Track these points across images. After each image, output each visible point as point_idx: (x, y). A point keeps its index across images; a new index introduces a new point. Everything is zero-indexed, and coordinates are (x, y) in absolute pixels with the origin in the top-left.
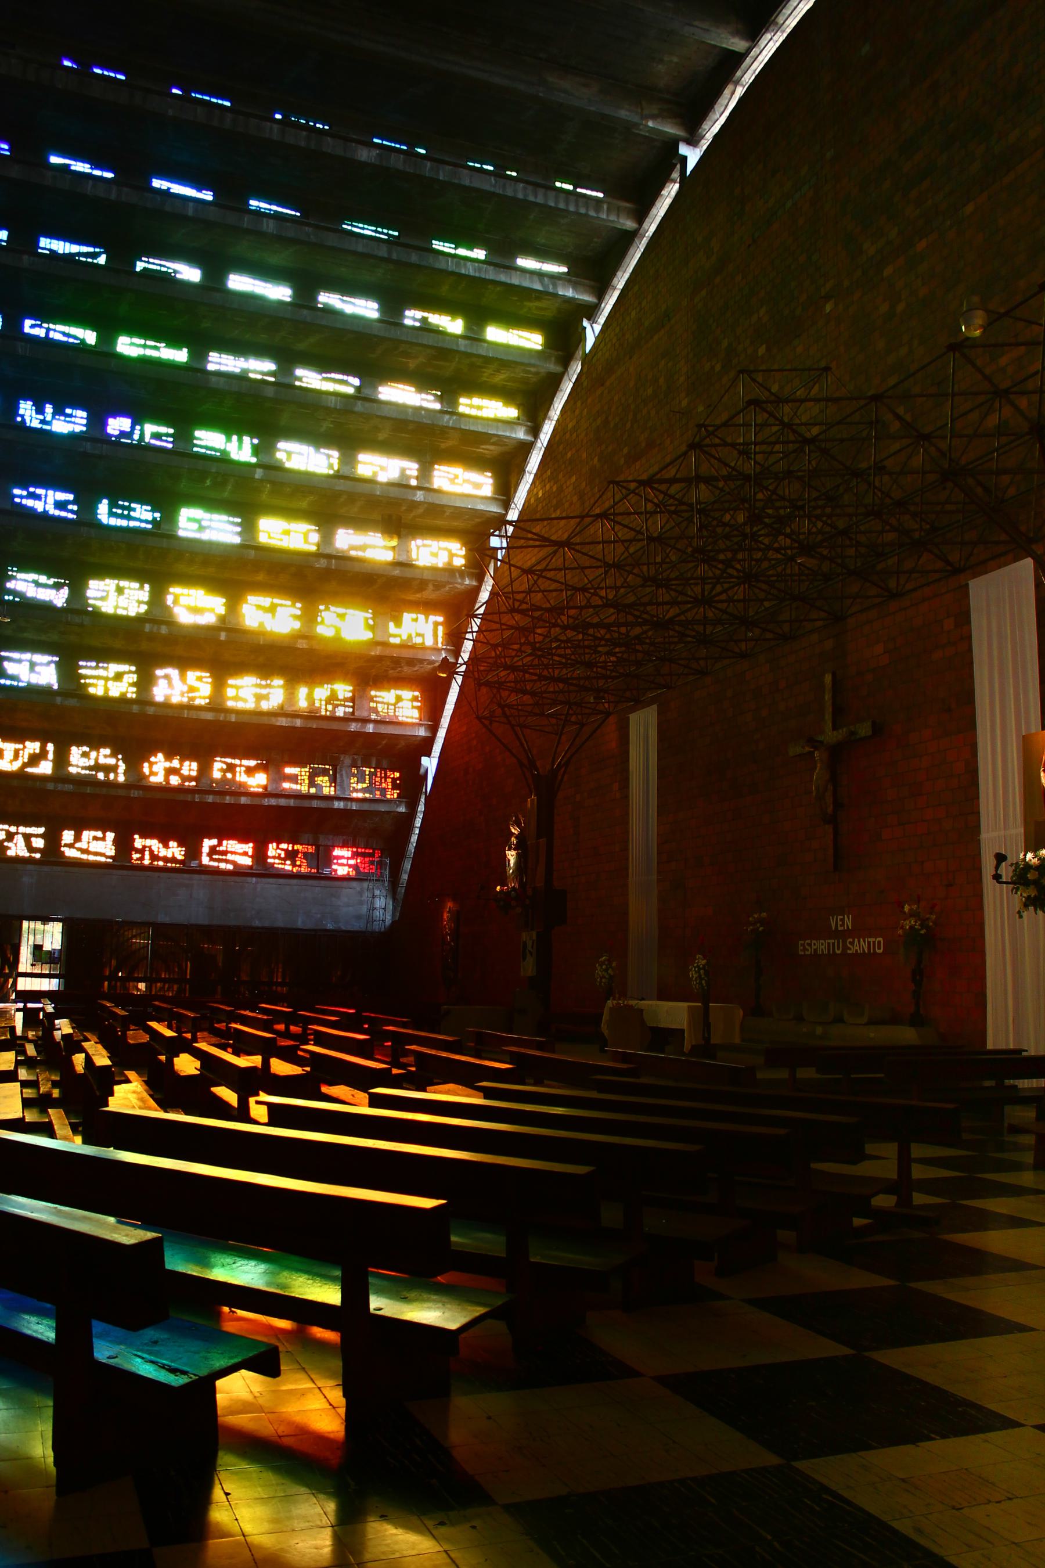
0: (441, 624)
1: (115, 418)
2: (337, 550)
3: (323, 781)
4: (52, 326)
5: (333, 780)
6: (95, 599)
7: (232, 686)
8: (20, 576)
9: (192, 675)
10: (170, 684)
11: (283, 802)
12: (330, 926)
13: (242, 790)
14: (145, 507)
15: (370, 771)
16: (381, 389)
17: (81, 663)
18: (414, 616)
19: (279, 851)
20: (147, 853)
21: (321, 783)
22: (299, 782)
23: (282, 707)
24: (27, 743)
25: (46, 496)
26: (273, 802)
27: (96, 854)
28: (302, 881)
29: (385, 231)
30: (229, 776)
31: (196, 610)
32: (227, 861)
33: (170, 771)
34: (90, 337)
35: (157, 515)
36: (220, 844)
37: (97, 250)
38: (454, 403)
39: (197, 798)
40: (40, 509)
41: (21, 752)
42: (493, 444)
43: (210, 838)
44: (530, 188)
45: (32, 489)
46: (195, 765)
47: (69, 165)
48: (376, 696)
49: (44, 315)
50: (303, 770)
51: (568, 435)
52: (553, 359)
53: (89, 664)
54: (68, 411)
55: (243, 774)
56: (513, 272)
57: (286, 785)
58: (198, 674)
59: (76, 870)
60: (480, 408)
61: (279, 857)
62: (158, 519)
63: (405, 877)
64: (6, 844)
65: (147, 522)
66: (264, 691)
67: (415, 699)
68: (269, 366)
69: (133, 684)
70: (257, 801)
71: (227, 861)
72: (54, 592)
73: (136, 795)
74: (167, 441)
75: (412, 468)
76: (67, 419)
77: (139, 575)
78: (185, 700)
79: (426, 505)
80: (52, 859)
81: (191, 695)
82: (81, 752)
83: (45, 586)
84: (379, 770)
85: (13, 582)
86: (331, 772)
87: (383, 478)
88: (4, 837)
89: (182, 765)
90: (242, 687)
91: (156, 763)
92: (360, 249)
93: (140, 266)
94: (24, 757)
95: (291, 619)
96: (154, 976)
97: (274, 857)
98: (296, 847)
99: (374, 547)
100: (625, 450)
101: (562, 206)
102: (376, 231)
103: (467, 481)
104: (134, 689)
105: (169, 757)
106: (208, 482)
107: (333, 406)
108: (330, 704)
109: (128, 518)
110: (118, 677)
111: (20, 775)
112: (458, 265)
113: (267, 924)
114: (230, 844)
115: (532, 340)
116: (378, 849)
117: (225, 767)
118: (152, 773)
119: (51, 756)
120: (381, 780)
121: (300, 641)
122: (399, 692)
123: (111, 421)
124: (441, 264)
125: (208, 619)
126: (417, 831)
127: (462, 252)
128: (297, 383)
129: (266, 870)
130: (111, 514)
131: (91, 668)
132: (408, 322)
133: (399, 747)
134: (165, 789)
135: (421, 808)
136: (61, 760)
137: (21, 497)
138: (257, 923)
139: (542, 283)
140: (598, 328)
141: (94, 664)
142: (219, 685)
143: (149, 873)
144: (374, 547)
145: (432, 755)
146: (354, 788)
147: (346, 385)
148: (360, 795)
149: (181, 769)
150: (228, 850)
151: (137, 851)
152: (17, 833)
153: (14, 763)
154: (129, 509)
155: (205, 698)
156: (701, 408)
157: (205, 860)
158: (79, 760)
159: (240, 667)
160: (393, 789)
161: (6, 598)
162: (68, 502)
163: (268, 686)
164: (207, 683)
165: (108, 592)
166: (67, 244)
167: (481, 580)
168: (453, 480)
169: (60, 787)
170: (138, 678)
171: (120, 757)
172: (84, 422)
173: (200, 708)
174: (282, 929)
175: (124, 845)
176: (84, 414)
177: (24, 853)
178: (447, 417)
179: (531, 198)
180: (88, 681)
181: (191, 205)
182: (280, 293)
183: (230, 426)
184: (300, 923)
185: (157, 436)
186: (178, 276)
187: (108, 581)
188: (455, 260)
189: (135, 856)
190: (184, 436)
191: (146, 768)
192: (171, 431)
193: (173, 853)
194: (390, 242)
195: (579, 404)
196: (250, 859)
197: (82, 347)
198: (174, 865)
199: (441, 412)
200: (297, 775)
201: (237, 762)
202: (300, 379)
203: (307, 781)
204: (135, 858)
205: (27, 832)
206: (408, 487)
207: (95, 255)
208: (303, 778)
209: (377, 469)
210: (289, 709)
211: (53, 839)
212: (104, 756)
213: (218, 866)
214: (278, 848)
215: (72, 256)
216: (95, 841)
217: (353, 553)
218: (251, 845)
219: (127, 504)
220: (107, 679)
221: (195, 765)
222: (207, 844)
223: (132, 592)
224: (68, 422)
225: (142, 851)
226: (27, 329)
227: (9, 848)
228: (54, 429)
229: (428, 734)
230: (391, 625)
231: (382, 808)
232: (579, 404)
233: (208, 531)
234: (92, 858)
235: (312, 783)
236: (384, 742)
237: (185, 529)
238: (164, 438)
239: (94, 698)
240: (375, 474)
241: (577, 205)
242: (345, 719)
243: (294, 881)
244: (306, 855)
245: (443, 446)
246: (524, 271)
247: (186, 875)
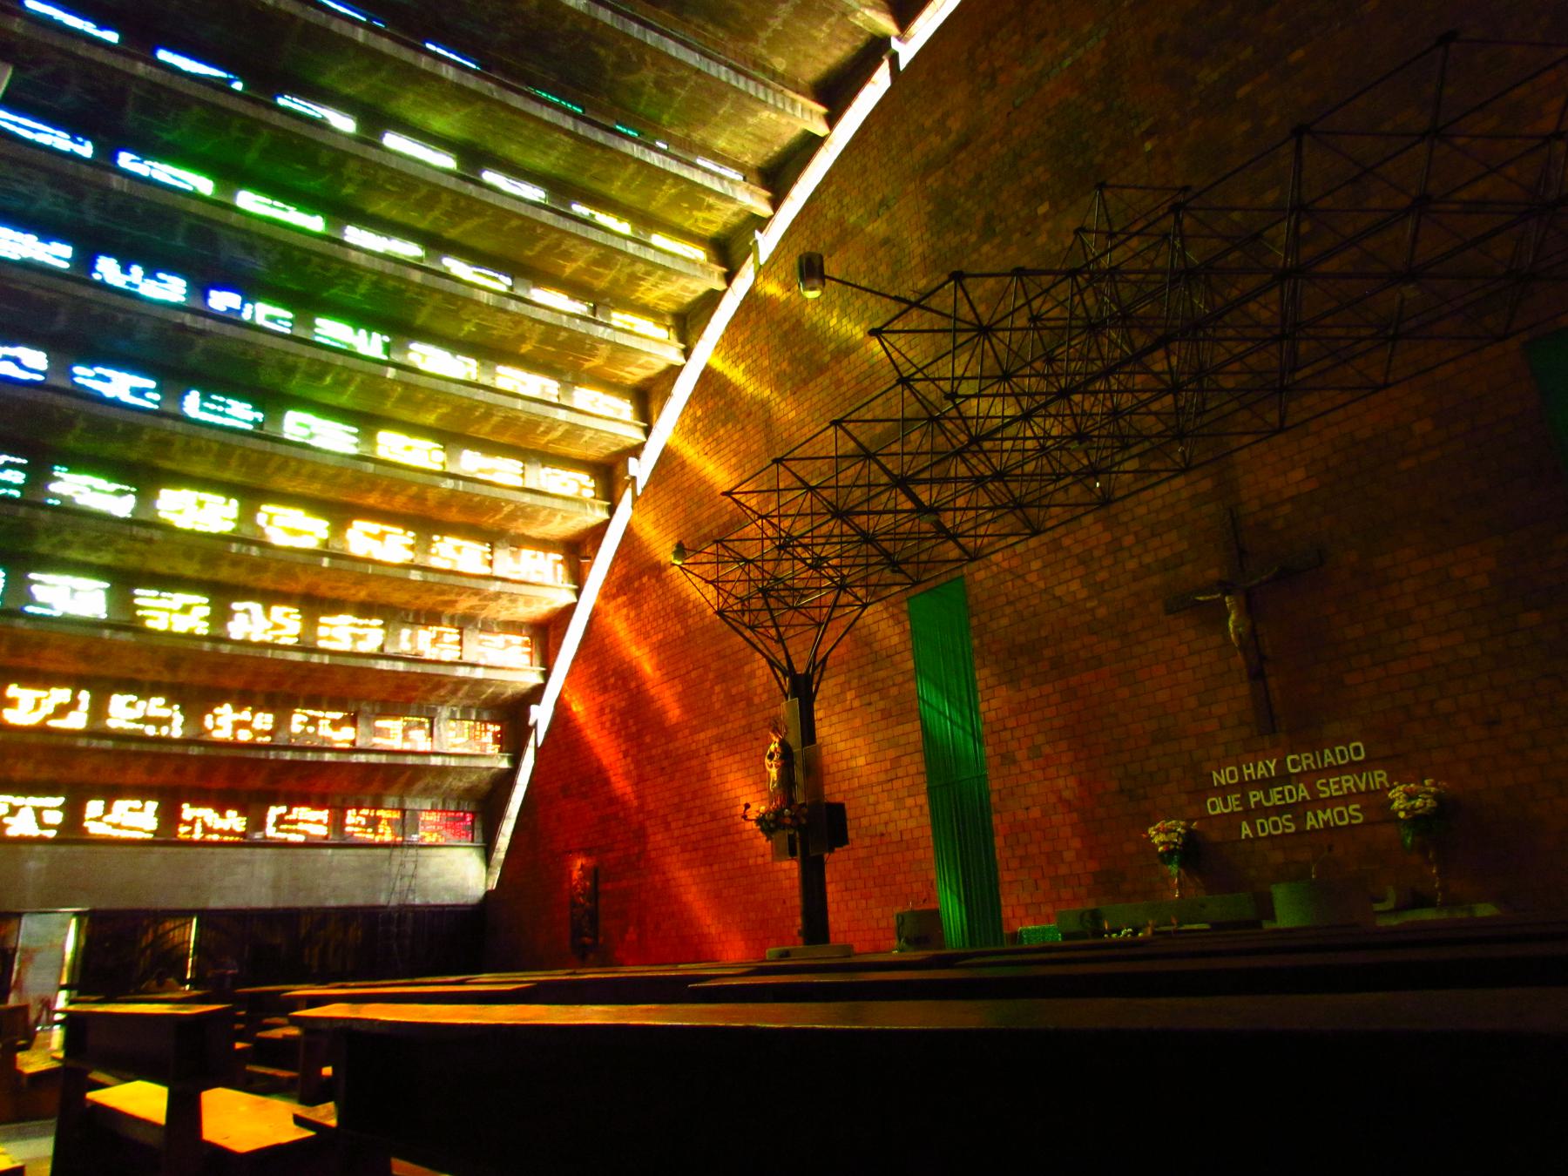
0: (562, 562)
4: (156, 164)
9: (278, 611)
11: (373, 758)
12: (418, 901)
13: (326, 745)
19: (359, 818)
24: (54, 691)
26: (362, 758)
27: (131, 829)
31: (295, 533)
34: (204, 185)
35: (260, 416)
36: (289, 812)
39: (272, 755)
41: (43, 702)
43: (277, 803)
44: (732, 73)
45: (100, 370)
49: (146, 150)
52: (716, 275)
54: (161, 276)
56: (695, 170)
59: (102, 848)
61: (359, 825)
69: (207, 619)
70: (343, 758)
71: (297, 832)
79: (567, 427)
86: (427, 726)
94: (48, 708)
97: (354, 825)
101: (761, 96)
104: (207, 624)
105: (238, 707)
106: (328, 380)
107: (485, 301)
109: (223, 414)
110: (186, 609)
111: (42, 730)
113: (344, 902)
114: (301, 812)
118: (216, 727)
125: (310, 543)
130: (202, 408)
133: (506, 696)
134: (236, 745)
136: (99, 709)
137: (85, 377)
138: (332, 903)
139: (722, 185)
142: (310, 620)
143: (200, 849)
149: (251, 722)
154: (224, 405)
157: (271, 831)
158: (124, 712)
159: (336, 606)
163: (367, 626)
169: (95, 743)
171: (177, 707)
175: (169, 816)
177: (34, 831)
178: (601, 329)
179: (734, 83)
184: (382, 900)
185: (273, 319)
192: (289, 315)
196: (326, 828)
201: (319, 714)
203: (400, 735)
210: (389, 650)
211: (74, 813)
212: (156, 706)
214: (358, 814)
218: (326, 812)
220: (171, 611)
225: (192, 823)
231: (483, 763)
235: (406, 737)
236: (490, 690)
238: (280, 322)
241: (775, 99)
247: (247, 850)
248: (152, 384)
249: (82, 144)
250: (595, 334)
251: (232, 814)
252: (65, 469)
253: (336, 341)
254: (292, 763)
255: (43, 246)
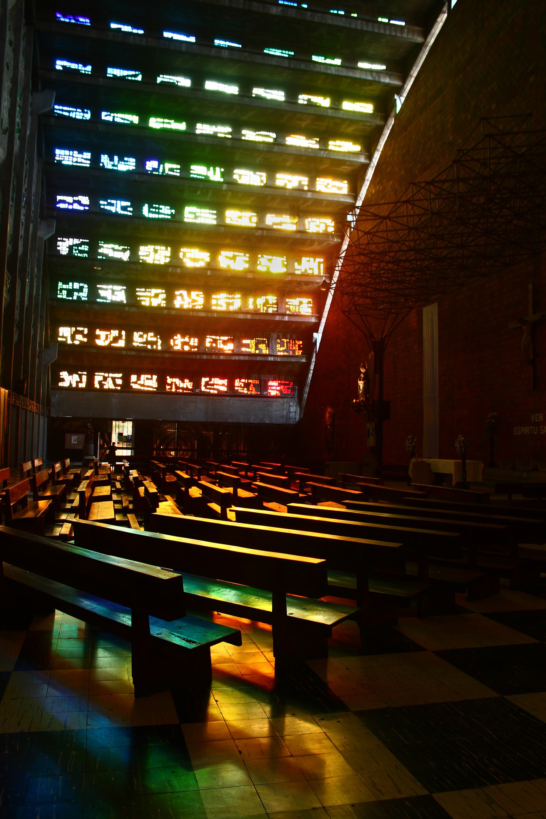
1: (150, 161)
2: (267, 226)
3: (262, 346)
4: (115, 115)
5: (268, 346)
6: (143, 256)
7: (214, 299)
8: (105, 246)
9: (194, 294)
10: (183, 299)
11: (242, 358)
12: (267, 422)
13: (221, 352)
14: (167, 207)
15: (287, 341)
16: (287, 139)
17: (137, 289)
18: (308, 259)
19: (240, 383)
20: (174, 386)
21: (261, 348)
22: (250, 347)
23: (240, 309)
24: (112, 331)
25: (116, 204)
26: (237, 358)
28: (253, 399)
29: (287, 52)
30: (214, 345)
31: (195, 260)
32: (214, 389)
33: (184, 344)
34: (135, 119)
35: (173, 211)
36: (210, 380)
37: (137, 73)
38: (327, 145)
39: (198, 357)
40: (114, 211)
41: (109, 336)
42: (348, 165)
43: (205, 378)
45: (109, 201)
46: (196, 340)
47: (120, 28)
48: (289, 302)
49: (112, 109)
50: (252, 341)
51: (387, 159)
52: (379, 118)
53: (141, 290)
54: (126, 159)
55: (221, 343)
56: (356, 71)
57: (244, 349)
58: (197, 293)
59: (138, 395)
60: (340, 146)
61: (241, 387)
62: (174, 213)
63: (306, 395)
64: (103, 382)
65: (168, 215)
66: (231, 301)
67: (309, 303)
68: (229, 129)
69: (164, 299)
70: (229, 358)
71: (214, 389)
72: (122, 253)
73: (167, 356)
74: (177, 172)
75: (305, 180)
76: (126, 163)
77: (165, 243)
78: (191, 306)
79: (312, 200)
80: (127, 390)
81: (193, 304)
82: (139, 335)
83: (118, 250)
84: (291, 340)
85: (102, 249)
87: (289, 186)
88: (102, 379)
89: (190, 340)
90: (220, 299)
91: (177, 339)
92: (274, 63)
93: (159, 80)
94: (111, 339)
95: (244, 263)
96: (179, 448)
97: (238, 387)
98: (249, 381)
99: (286, 223)
100: (419, 166)
102: (282, 53)
103: (334, 186)
104: (165, 302)
105: (183, 336)
106: (199, 193)
107: (262, 149)
108: (265, 306)
109: (159, 213)
110: (156, 296)
112: (326, 69)
113: (235, 421)
114: (216, 381)
115: (367, 108)
116: (292, 381)
117: (212, 340)
118: (175, 345)
119: (124, 337)
120: (293, 345)
121: (249, 274)
122: (301, 299)
123: (148, 163)
124: (318, 69)
125: (201, 264)
126: (312, 372)
127: (329, 61)
128: (243, 138)
129: (234, 393)
130: (150, 212)
131: (142, 292)
132: (300, 102)
133: (302, 328)
134: (182, 353)
135: (314, 359)
136: (129, 339)
137: (104, 205)
138: (230, 420)
139: (372, 76)
140: (403, 99)
141: (144, 290)
142: (208, 298)
143: (175, 396)
144: (286, 223)
145: (319, 332)
146: (278, 350)
147: (269, 137)
148: (282, 354)
149: (189, 342)
150: (215, 383)
151: (169, 385)
152: (109, 377)
153: (106, 341)
154: (159, 208)
155: (200, 305)
156: (460, 141)
157: (203, 389)
158: (138, 339)
160: (299, 350)
161: (99, 257)
162: (127, 207)
163: (233, 298)
164: (201, 297)
165: (149, 252)
166: (122, 70)
167: (342, 238)
168: (326, 186)
170: (166, 296)
171: (158, 337)
172: (134, 164)
173: (198, 311)
174: (243, 423)
175: (162, 382)
176: (134, 160)
177: (112, 387)
178: (323, 152)
180: (141, 298)
181: (184, 45)
182: (232, 90)
183: (209, 162)
184: (252, 421)
185: (172, 170)
186: (179, 84)
187: (149, 246)
188: (325, 66)
189: (168, 387)
190: (185, 169)
191: (172, 342)
192: (179, 167)
193: (187, 386)
194: (290, 58)
195: (393, 142)
196: (226, 388)
197: (131, 125)
198: (187, 391)
199: (320, 149)
200: (249, 344)
201: (218, 338)
202: (244, 135)
203: (254, 347)
204: (168, 388)
205: (113, 376)
206: (303, 190)
207: (136, 76)
208: (252, 345)
209: (286, 182)
210: (244, 310)
212: (151, 336)
213: (210, 392)
214: (240, 381)
215: (124, 77)
216: (147, 380)
217: (275, 227)
218: (226, 380)
219: (157, 206)
220: (150, 297)
221: (196, 340)
222: (204, 380)
223: (161, 251)
224: (126, 165)
225: (171, 385)
226: (103, 118)
227: (105, 385)
228: (119, 169)
229: (317, 321)
230: (296, 264)
231: (293, 360)
232: (393, 142)
233: (199, 218)
234: (146, 389)
235: (257, 348)
236: (294, 326)
237: (188, 218)
238: (175, 171)
239: (144, 307)
240: (286, 184)
242: (273, 314)
243: (249, 399)
244: (254, 385)
245: (321, 168)
246: (362, 70)
247: (193, 397)
248: (129, 204)
249: (87, 113)
250: (319, 156)
251: (186, 381)
252: (102, 242)
253: (200, 175)
254: (207, 360)
255: (80, 156)
